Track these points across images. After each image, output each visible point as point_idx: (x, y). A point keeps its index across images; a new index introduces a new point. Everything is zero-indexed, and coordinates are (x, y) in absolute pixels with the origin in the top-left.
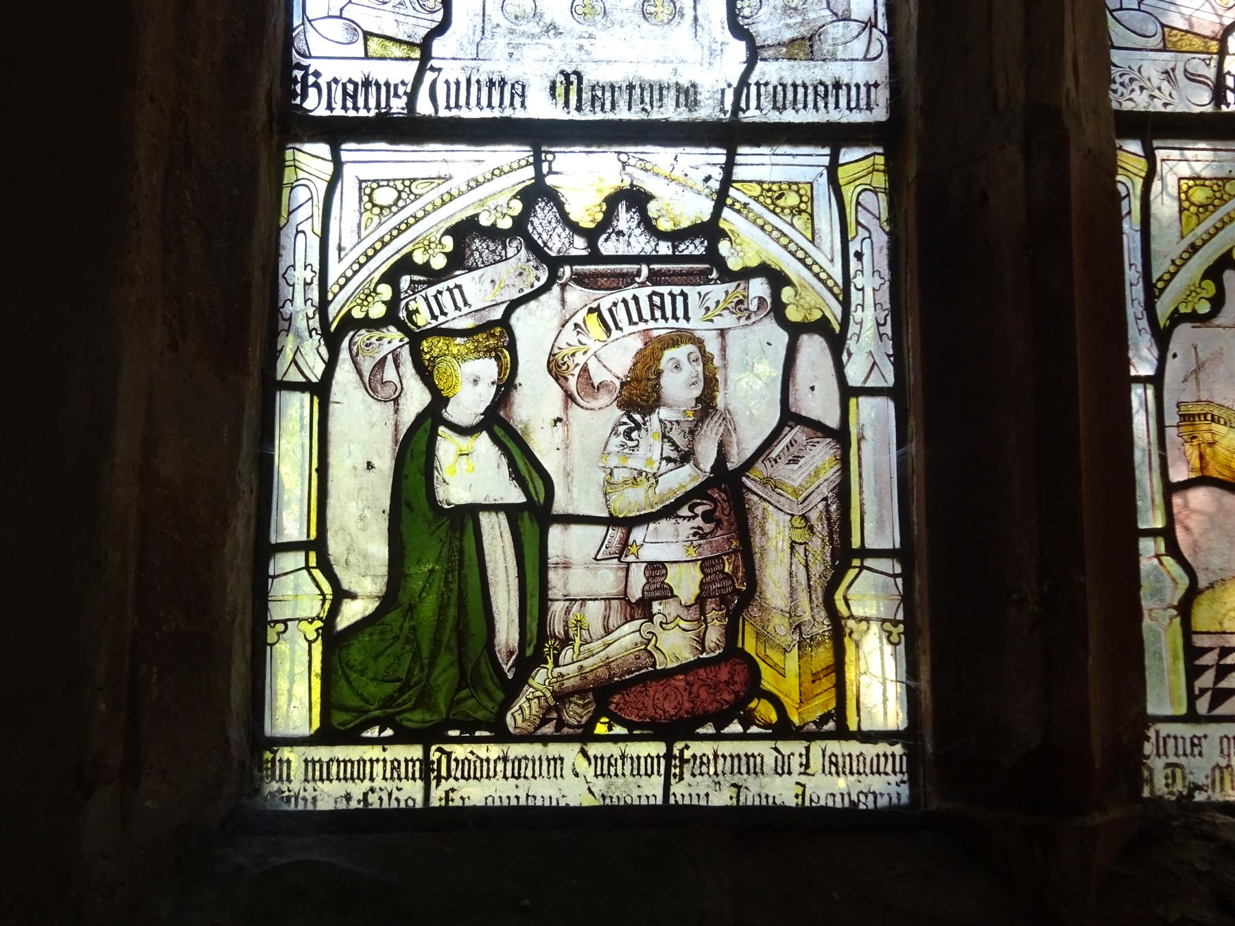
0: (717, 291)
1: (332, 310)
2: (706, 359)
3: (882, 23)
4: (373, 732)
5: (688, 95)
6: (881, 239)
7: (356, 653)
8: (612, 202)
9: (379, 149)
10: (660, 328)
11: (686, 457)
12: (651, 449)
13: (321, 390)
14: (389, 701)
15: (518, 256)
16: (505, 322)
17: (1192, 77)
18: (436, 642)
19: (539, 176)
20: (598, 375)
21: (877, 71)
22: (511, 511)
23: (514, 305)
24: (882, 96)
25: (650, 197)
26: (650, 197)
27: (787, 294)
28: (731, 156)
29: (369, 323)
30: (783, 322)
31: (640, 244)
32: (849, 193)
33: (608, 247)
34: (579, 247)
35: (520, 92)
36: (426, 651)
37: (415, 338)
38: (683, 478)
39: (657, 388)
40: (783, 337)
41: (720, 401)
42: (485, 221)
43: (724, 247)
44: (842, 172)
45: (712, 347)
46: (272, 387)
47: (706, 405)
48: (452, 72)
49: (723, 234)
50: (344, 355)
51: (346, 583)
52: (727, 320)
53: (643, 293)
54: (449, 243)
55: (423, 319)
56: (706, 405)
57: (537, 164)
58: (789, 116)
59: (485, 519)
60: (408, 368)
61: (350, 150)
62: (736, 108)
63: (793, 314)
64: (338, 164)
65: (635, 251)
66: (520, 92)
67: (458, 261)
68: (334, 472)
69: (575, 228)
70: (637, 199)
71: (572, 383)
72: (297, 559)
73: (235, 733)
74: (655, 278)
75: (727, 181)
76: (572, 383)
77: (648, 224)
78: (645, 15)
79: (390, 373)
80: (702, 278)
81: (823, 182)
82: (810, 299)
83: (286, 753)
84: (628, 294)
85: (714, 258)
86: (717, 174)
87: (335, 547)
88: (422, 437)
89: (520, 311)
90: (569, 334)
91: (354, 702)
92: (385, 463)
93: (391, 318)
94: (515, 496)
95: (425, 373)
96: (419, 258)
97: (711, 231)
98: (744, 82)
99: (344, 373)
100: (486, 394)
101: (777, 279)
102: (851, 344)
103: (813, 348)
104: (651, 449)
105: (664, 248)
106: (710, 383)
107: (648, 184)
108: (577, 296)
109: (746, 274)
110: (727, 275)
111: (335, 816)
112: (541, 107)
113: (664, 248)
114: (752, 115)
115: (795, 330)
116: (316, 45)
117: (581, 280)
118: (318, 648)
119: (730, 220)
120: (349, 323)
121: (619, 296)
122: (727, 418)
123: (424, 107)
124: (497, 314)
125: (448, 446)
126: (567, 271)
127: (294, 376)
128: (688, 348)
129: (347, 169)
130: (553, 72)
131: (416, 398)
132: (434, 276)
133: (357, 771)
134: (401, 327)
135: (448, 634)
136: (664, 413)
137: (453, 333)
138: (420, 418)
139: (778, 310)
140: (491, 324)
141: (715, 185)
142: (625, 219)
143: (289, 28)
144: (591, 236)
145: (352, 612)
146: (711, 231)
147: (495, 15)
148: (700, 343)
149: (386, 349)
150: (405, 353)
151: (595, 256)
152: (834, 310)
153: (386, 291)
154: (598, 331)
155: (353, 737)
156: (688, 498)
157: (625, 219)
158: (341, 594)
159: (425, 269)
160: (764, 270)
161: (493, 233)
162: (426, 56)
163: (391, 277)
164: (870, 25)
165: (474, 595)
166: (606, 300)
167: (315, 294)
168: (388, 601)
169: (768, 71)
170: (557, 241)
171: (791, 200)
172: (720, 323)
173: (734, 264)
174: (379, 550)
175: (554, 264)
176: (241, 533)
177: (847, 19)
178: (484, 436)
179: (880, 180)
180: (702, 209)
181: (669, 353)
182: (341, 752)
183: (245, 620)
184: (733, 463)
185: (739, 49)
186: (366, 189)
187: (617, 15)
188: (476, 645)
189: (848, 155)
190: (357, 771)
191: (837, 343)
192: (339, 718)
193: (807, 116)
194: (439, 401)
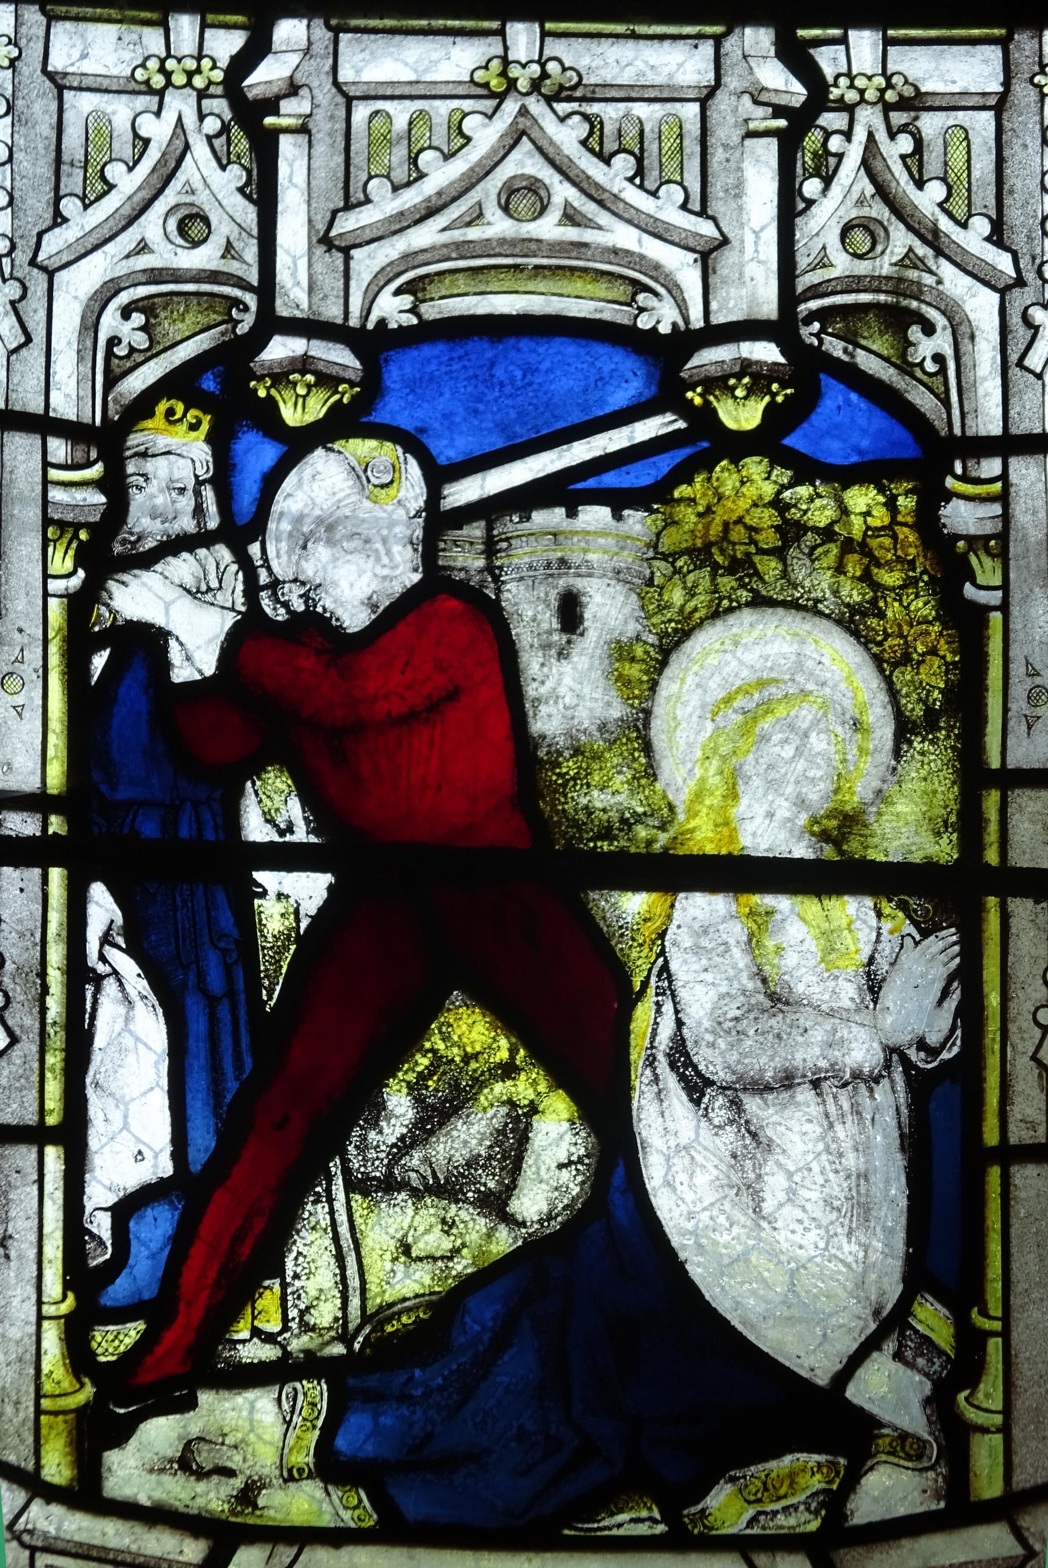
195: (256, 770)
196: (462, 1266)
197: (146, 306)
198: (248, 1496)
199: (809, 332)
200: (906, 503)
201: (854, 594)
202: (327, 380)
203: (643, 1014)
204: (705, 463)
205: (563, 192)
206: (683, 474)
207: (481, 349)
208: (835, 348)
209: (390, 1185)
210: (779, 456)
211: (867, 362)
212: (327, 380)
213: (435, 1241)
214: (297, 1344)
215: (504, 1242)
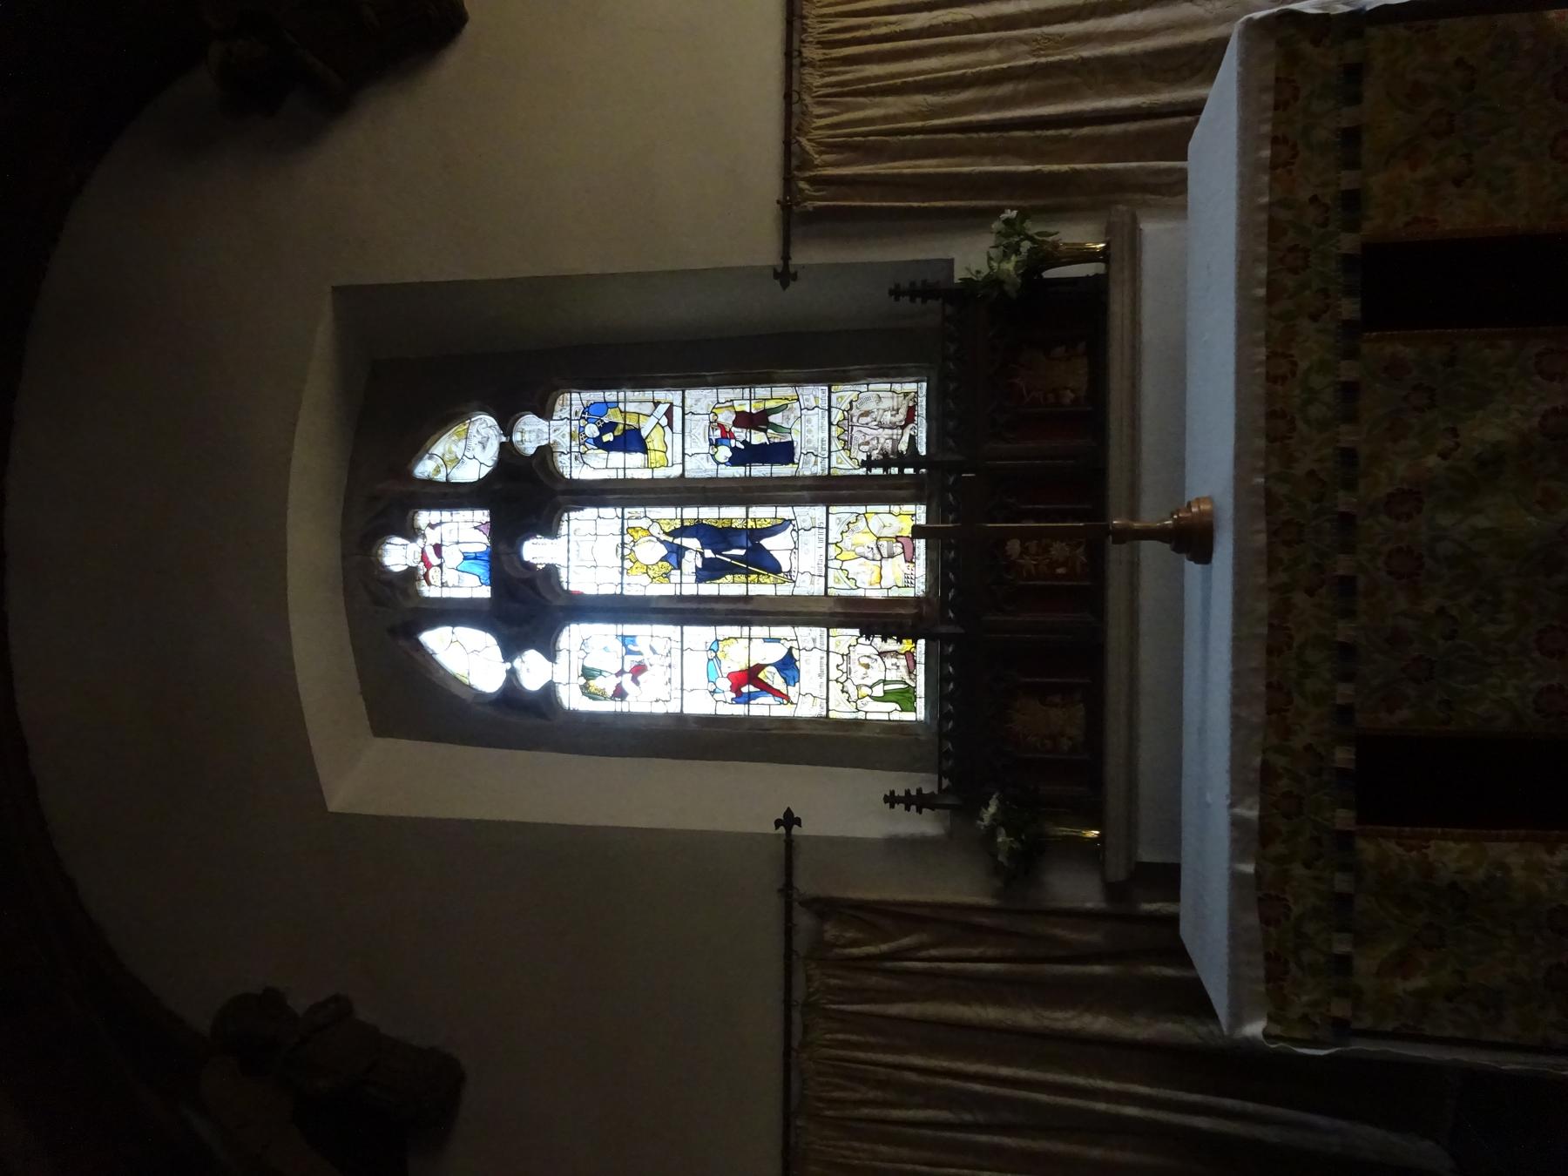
5: (822, 658)
10: (857, 663)
11: (876, 660)
13: (866, 712)
24: (822, 629)
34: (845, 675)
46: (866, 719)
47: (869, 657)
56: (869, 657)
70: (838, 666)
85: (847, 655)
97: (843, 655)
101: (850, 646)
120: (857, 708)
131: (868, 698)
142: (840, 668)
146: (843, 655)
155: (915, 708)
161: (843, 687)
168: (897, 703)
169: (818, 645)
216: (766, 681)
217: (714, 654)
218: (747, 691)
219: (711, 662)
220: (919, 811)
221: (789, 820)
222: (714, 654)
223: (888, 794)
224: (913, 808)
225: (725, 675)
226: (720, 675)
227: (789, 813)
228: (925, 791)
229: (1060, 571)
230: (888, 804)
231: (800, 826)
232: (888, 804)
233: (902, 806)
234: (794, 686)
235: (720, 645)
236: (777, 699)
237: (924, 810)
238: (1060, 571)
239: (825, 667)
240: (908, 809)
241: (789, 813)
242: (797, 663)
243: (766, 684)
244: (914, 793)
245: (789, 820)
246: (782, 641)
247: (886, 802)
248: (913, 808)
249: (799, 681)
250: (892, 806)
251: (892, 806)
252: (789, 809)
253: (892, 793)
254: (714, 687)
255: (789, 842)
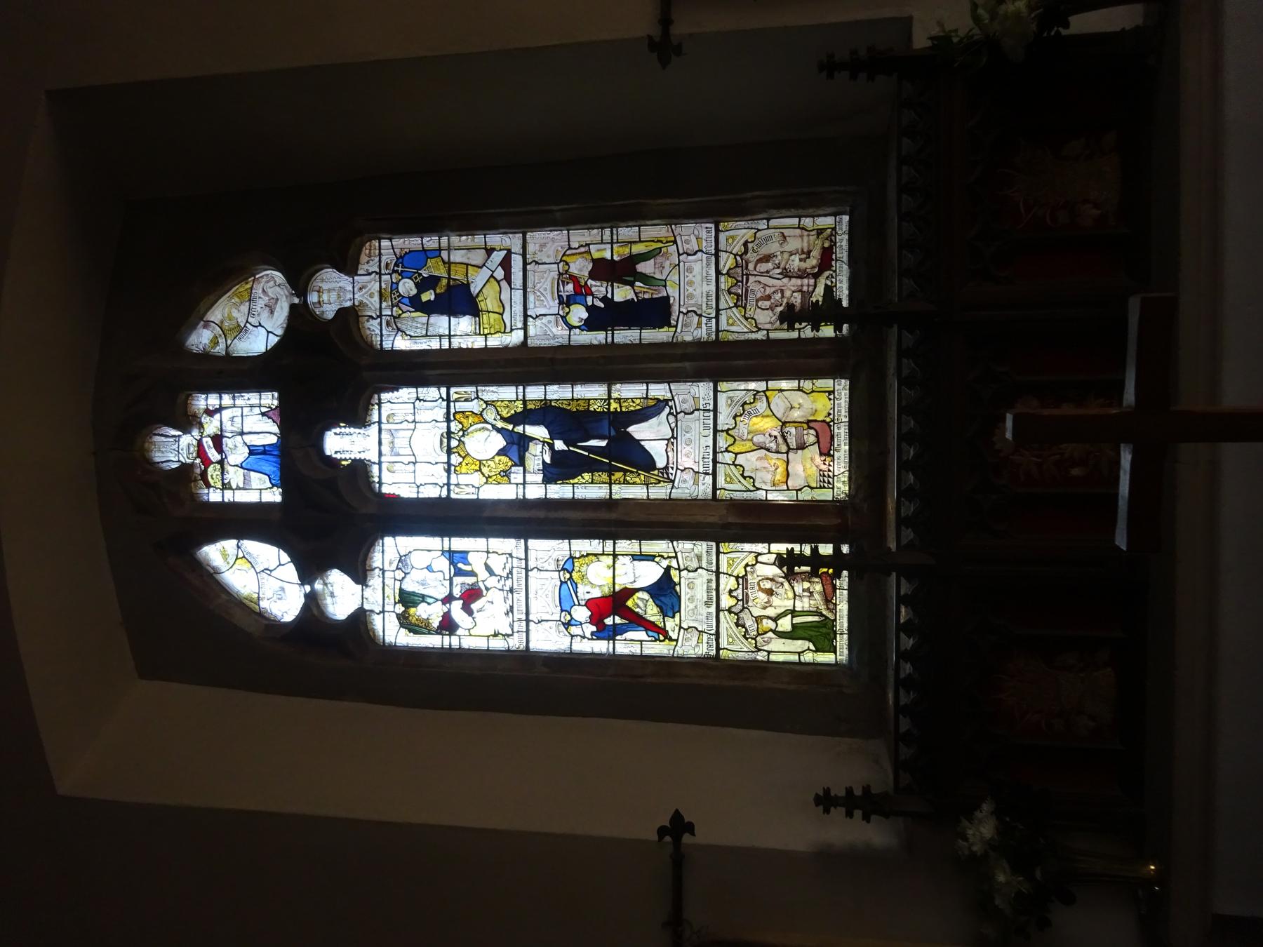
0: (749, 577)
1: (753, 650)
2: (763, 579)
3: (694, 542)
4: (835, 644)
5: (709, 581)
6: (739, 544)
7: (820, 647)
8: (731, 596)
9: (721, 640)
10: (757, 588)
11: (782, 584)
12: (780, 591)
13: (769, 652)
14: (829, 640)
15: (741, 615)
16: (755, 617)
17: (704, 480)
18: (818, 632)
19: (726, 610)
20: (766, 600)
21: (704, 544)
22: (793, 617)
23: (752, 616)
24: (710, 543)
25: (730, 589)
26: (730, 589)
27: (750, 564)
28: (722, 573)
29: (756, 644)
30: (755, 564)
31: (740, 591)
32: (729, 551)
33: (740, 598)
34: (741, 603)
35: (709, 613)
36: (818, 634)
37: (759, 634)
38: (786, 585)
39: (769, 589)
40: (758, 564)
41: (771, 577)
42: (735, 621)
43: (741, 575)
44: (726, 551)
45: (760, 578)
46: (768, 661)
47: (772, 580)
48: (705, 626)
49: (738, 575)
50: (762, 648)
51: (806, 648)
52: (755, 575)
53: (750, 591)
54: (740, 628)
55: (755, 633)
56: (772, 580)
57: (723, 610)
58: (714, 562)
59: (794, 622)
60: (764, 636)
61: (721, 646)
62: (712, 571)
63: (754, 562)
64: (724, 649)
65: (741, 592)
66: (709, 613)
67: (743, 626)
68: (785, 650)
69: (737, 604)
70: (731, 591)
71: (767, 605)
72: (802, 657)
73: (834, 668)
74: (747, 589)
75: (727, 574)
76: (767, 605)
77: (735, 590)
78: (693, 589)
79: (766, 639)
80: (747, 580)
81: (727, 555)
82: (750, 559)
83: (838, 660)
84: (750, 594)
85: (743, 577)
86: (725, 575)
87: (799, 650)
88: (780, 634)
89: (753, 614)
90: (758, 605)
91: (829, 647)
92: (783, 640)
93: (755, 639)
94: (790, 615)
95: (766, 633)
96: (743, 634)
97: (737, 578)
98: (707, 570)
99: (765, 648)
100: (770, 621)
101: (747, 565)
102: (760, 552)
103: (760, 559)
104: (780, 591)
105: (741, 586)
106: (767, 579)
107: (728, 589)
108: (750, 604)
109: (746, 571)
110: (746, 575)
111: (849, 651)
112: (713, 609)
113: (741, 586)
114: (714, 569)
115: (757, 562)
116: (700, 652)
117: (747, 603)
118: (819, 653)
119: (735, 574)
120: (756, 647)
121: (750, 596)
122: (774, 576)
123: (713, 632)
124: (754, 619)
125: (780, 629)
126: (745, 606)
127: (766, 657)
128: (760, 583)
129: (726, 647)
130: (704, 607)
131: (771, 634)
132: (746, 630)
133: (842, 647)
134: (756, 637)
135: (816, 630)
136: (773, 588)
137: (758, 627)
138: (774, 634)
139: (753, 565)
140: (756, 620)
141: (728, 576)
142: (735, 594)
143: (697, 658)
144: (738, 600)
145: (812, 647)
146: (737, 578)
147: (693, 618)
148: (760, 581)
149: (761, 640)
150: (762, 636)
151: (742, 600)
152: (753, 555)
153: (750, 640)
154: (757, 600)
155: (836, 647)
156: (790, 584)
157: (735, 594)
158: (809, 649)
159: (745, 633)
160: (745, 568)
161: (738, 619)
162: (702, 631)
163: (747, 639)
164: (694, 544)
165: (809, 624)
166: (751, 598)
167: (750, 653)
168: (810, 640)
169: (704, 565)
170: (739, 607)
171: (731, 562)
172: (756, 576)
173: (744, 573)
174: (800, 642)
175: (744, 608)
176: (798, 668)
177: (693, 549)
178: (778, 622)
179: (727, 544)
180: (733, 579)
181: (762, 586)
182: (838, 649)
183: (813, 667)
184: (783, 575)
185: (700, 570)
186: (729, 643)
187: (693, 594)
188: (819, 624)
189: (721, 550)
190: (842, 647)
191: (760, 554)
192: (832, 650)
193: (714, 558)
194: (771, 630)
195: (604, 623)
196: (653, 604)
197: (559, 632)
198: (677, 625)
199: (560, 569)
200: (576, 560)
201: (585, 565)
202: (566, 615)
203: (628, 587)
204: (573, 579)
205: (547, 592)
206: (574, 581)
207: (562, 601)
208: (561, 567)
209: (645, 611)
210: (572, 572)
211: (563, 563)
212: (566, 615)
213: (651, 607)
214: (662, 620)
215: (651, 600)
216: (637, 610)
217: (568, 576)
218: (611, 623)
219: (564, 586)
220: (866, 818)
221: (678, 826)
222: (568, 576)
223: (821, 793)
224: (858, 814)
225: (583, 603)
226: (577, 603)
227: (677, 816)
228: (875, 790)
229: (1076, 472)
230: (821, 808)
231: (693, 834)
232: (821, 808)
233: (842, 810)
234: (673, 617)
235: (576, 564)
236: (650, 633)
237: (873, 817)
238: (1076, 472)
239: (714, 593)
240: (849, 814)
241: (677, 816)
242: (677, 588)
243: (637, 614)
244: (858, 792)
245: (678, 826)
246: (657, 559)
247: (817, 805)
248: (858, 814)
249: (679, 611)
250: (827, 811)
251: (827, 811)
252: (677, 811)
253: (827, 791)
254: (568, 618)
255: (678, 860)
